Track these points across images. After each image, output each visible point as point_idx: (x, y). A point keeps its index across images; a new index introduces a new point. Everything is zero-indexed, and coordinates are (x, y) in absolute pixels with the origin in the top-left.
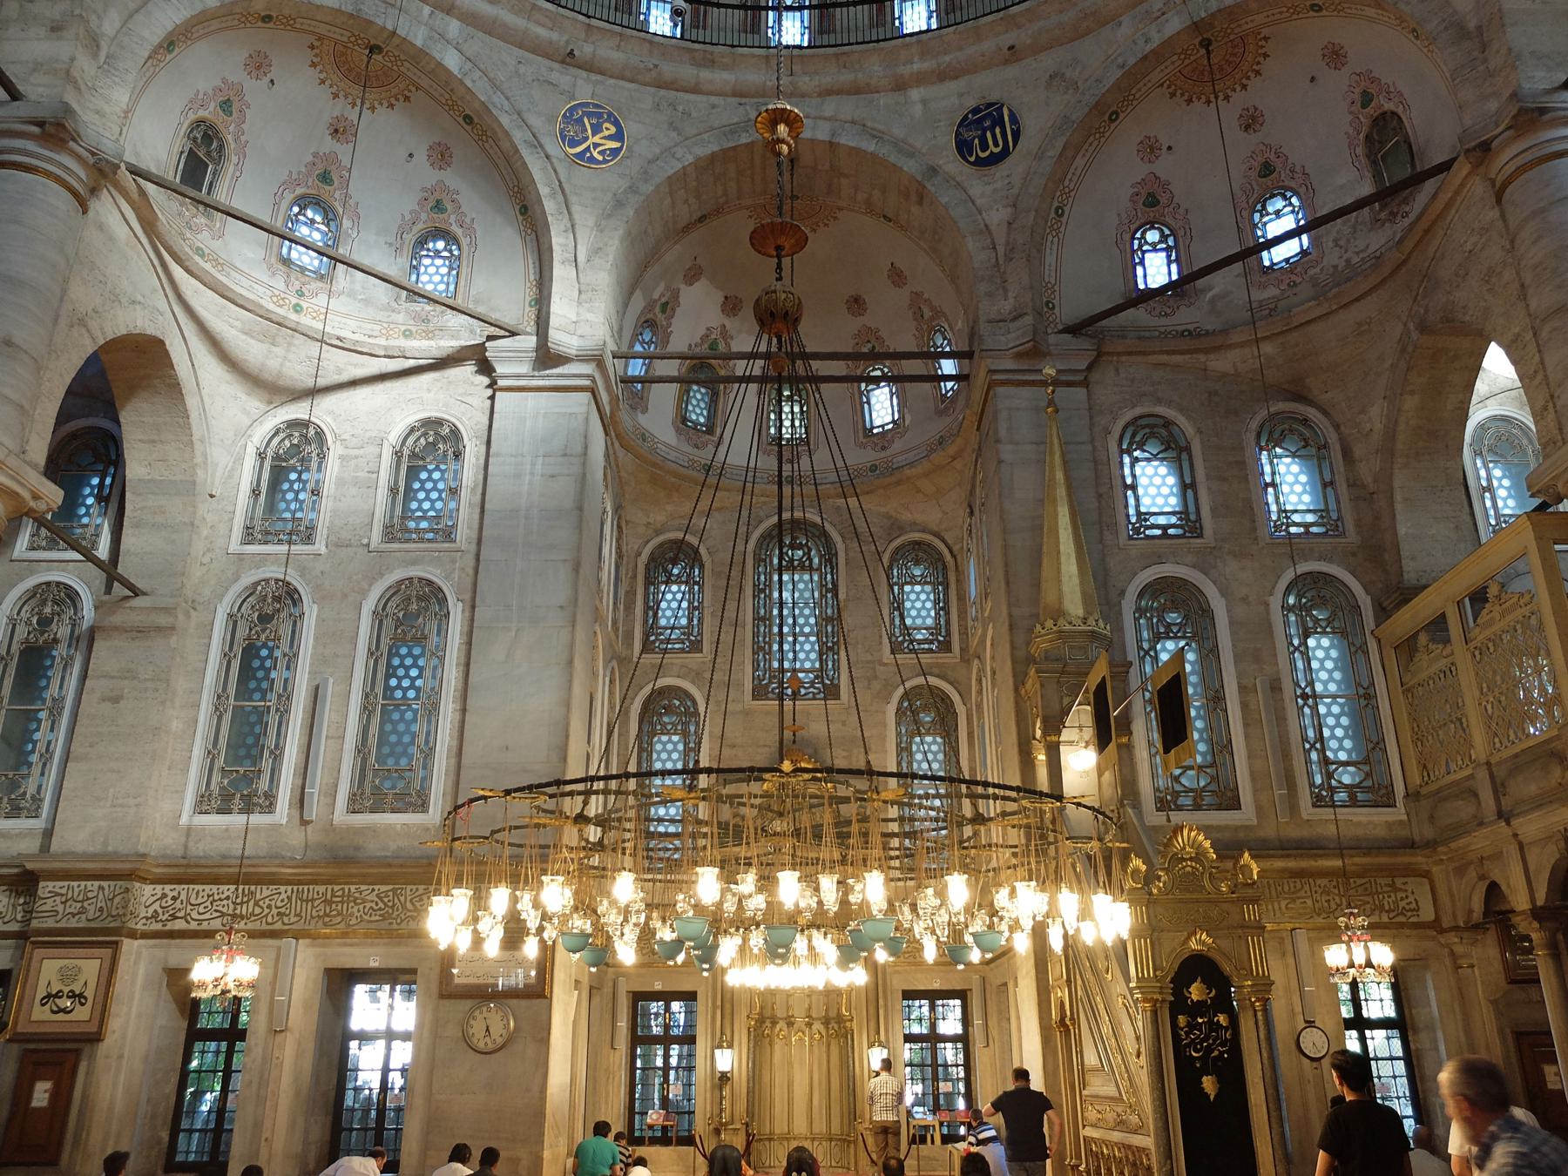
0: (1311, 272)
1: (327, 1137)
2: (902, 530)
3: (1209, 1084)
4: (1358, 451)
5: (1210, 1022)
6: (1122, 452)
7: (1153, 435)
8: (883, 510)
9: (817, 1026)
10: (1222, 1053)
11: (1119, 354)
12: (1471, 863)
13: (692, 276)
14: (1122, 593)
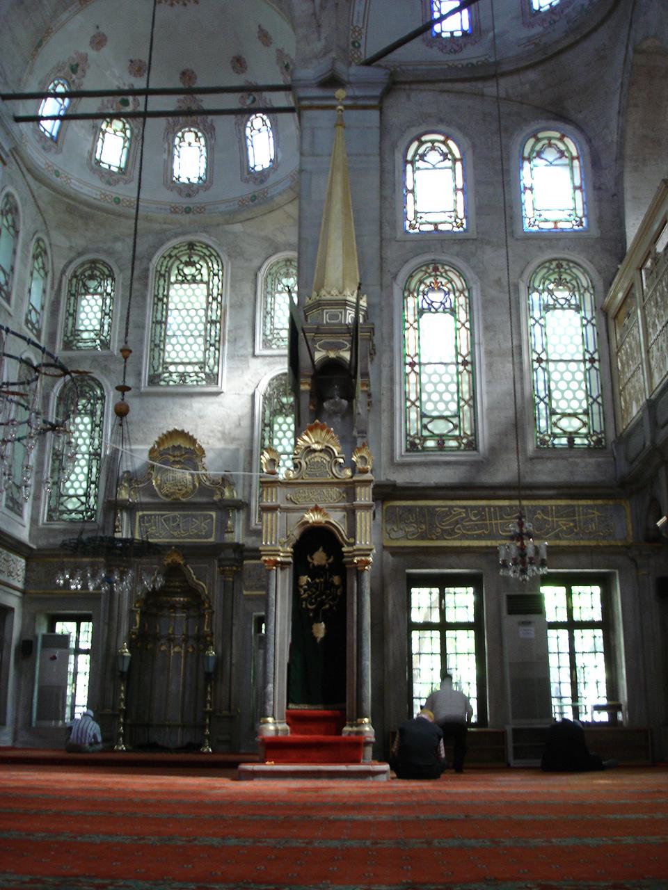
0: (566, 11)
5: (326, 582)
6: (406, 162)
7: (433, 148)
8: (262, 233)
9: (191, 642)
10: (331, 606)
11: (411, 83)
13: (99, 41)
14: (395, 277)
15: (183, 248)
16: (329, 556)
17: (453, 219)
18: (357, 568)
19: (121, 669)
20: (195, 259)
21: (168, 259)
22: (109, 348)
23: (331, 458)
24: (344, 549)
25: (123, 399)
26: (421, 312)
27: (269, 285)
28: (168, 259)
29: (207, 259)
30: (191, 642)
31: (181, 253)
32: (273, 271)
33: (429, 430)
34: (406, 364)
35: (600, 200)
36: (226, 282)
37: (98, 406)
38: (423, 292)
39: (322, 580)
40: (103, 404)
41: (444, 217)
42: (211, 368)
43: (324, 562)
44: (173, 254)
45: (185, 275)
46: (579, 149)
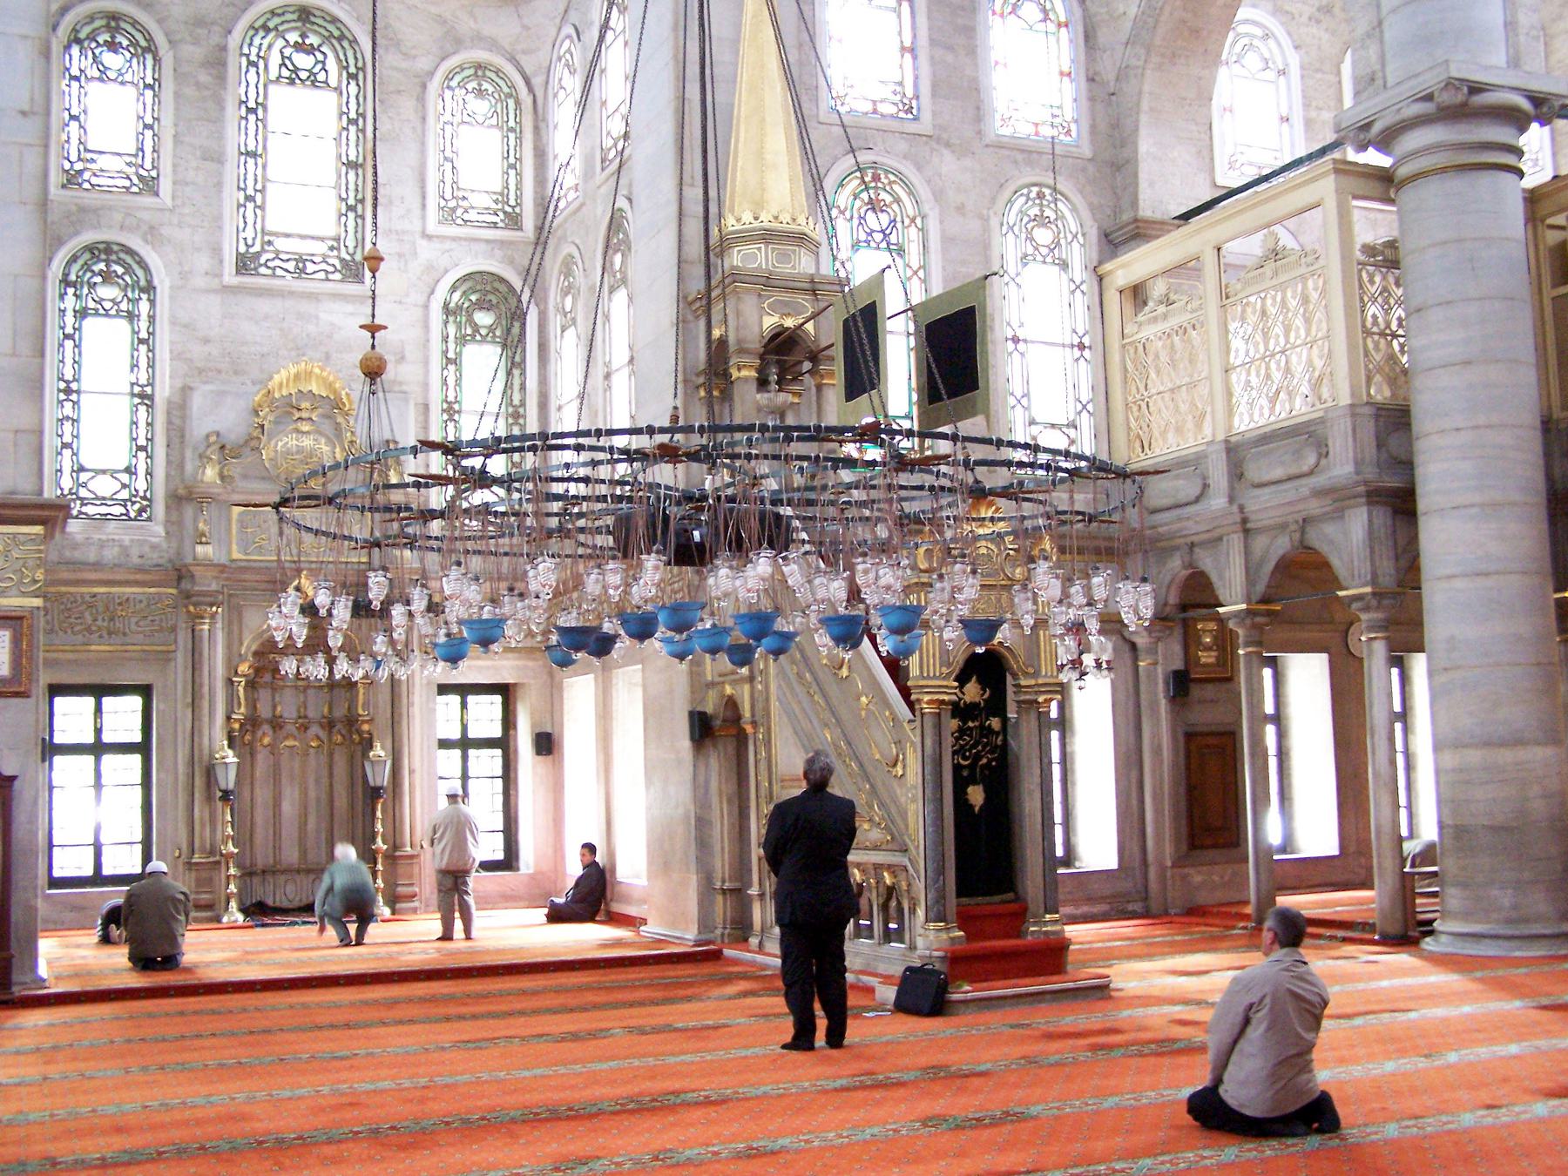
1: (1398, 886)
2: (458, 43)
3: (976, 795)
4: (1103, 36)
5: (982, 727)
8: (434, 10)
9: (315, 729)
10: (990, 761)
12: (1177, 548)
15: (289, 17)
17: (898, 97)
19: (223, 787)
20: (313, 40)
21: (262, 33)
22: (157, 195)
25: (373, 347)
28: (262, 33)
29: (335, 42)
30: (315, 729)
31: (286, 26)
35: (1092, 99)
37: (144, 306)
40: (152, 302)
41: (886, 92)
42: (351, 250)
44: (271, 25)
45: (296, 70)
46: (1068, 11)
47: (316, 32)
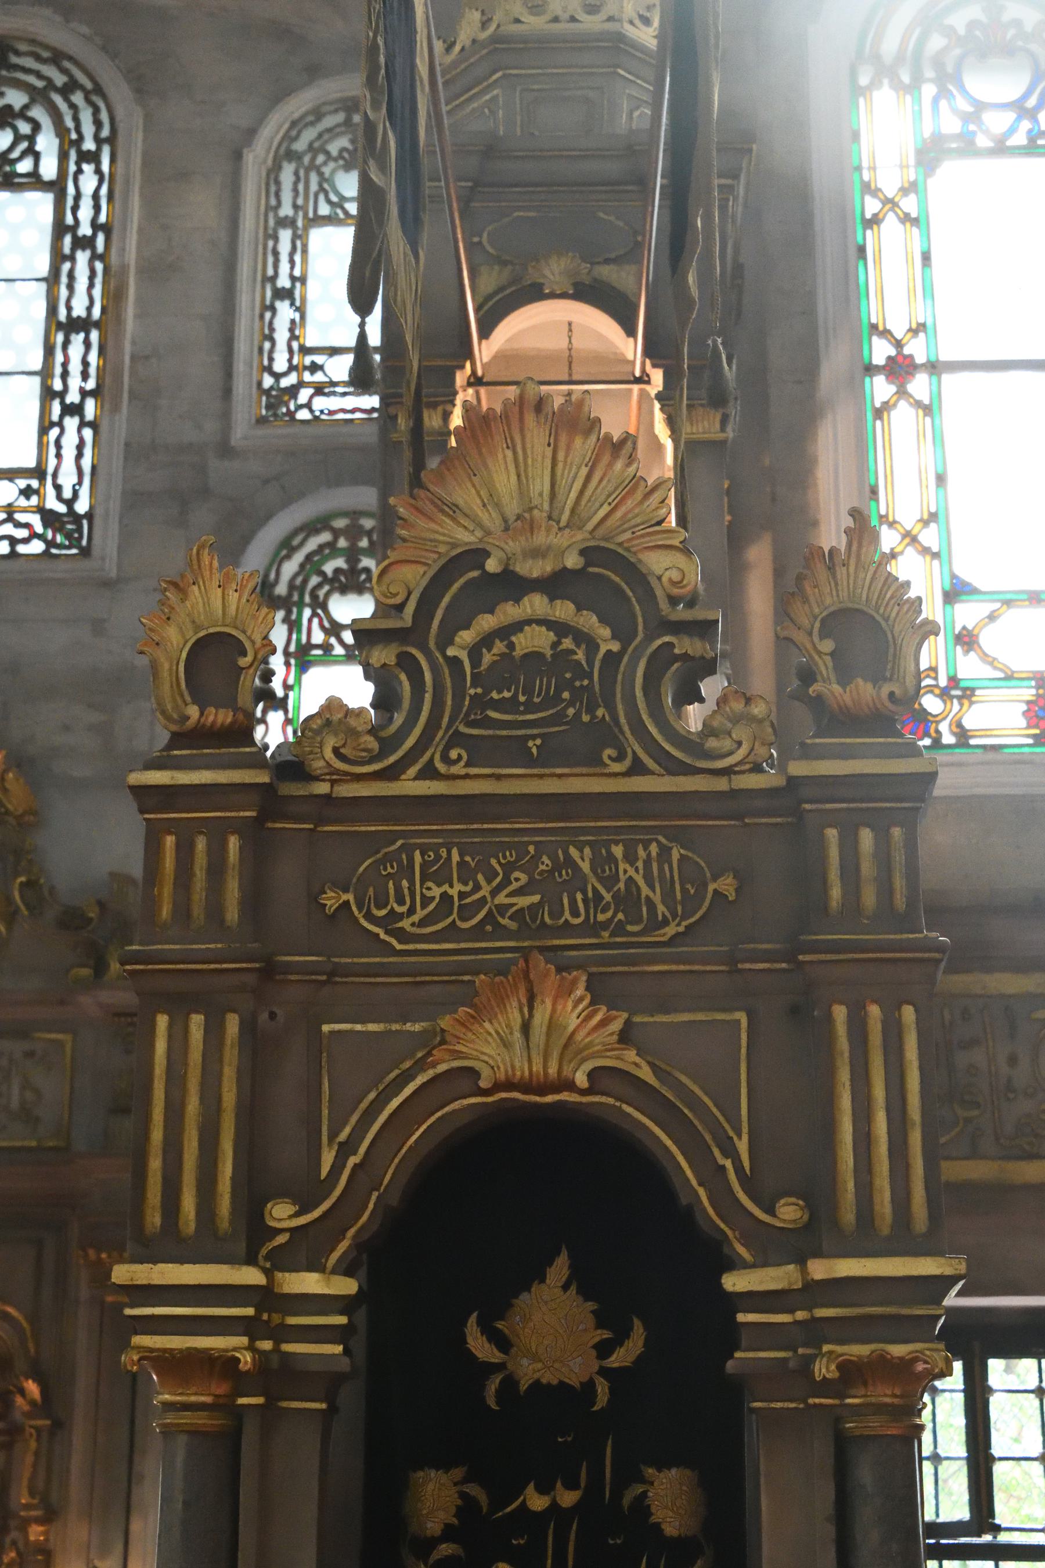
16: (613, 1322)
18: (838, 1420)
23: (623, 634)
24: (734, 1282)
26: (930, 154)
27: (287, 197)
32: (300, 146)
33: (985, 657)
34: (870, 369)
36: (127, 182)
38: (938, 63)
39: (568, 1498)
42: (67, 494)
43: (575, 1367)
47: (18, 85)
